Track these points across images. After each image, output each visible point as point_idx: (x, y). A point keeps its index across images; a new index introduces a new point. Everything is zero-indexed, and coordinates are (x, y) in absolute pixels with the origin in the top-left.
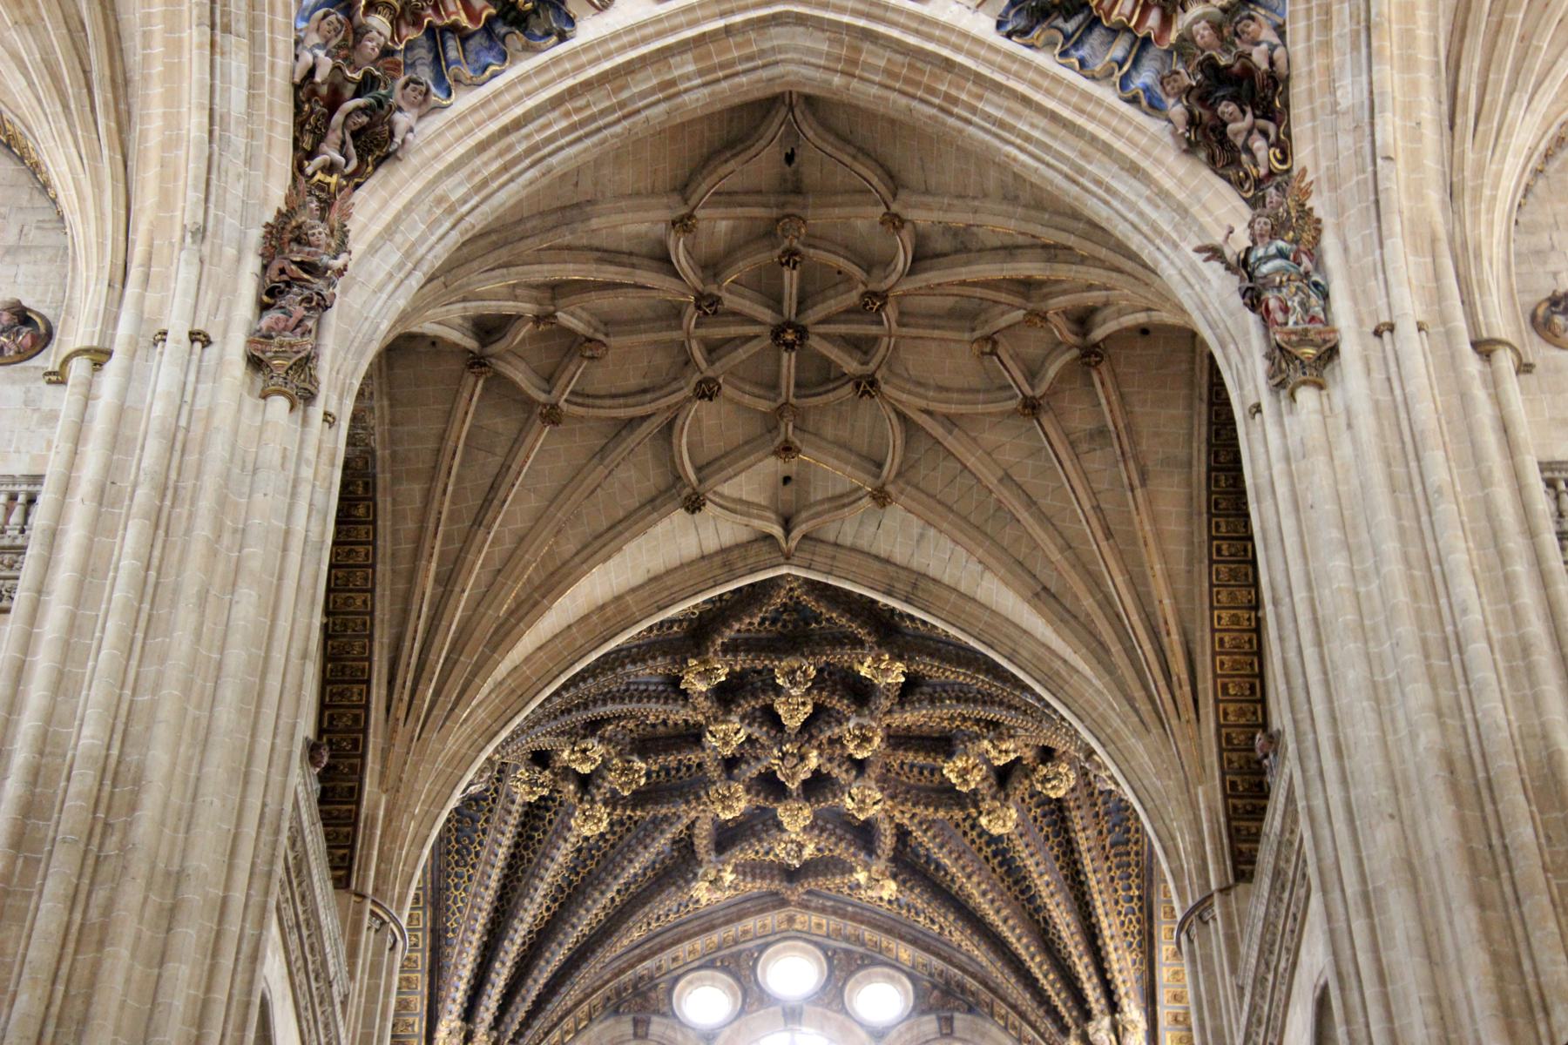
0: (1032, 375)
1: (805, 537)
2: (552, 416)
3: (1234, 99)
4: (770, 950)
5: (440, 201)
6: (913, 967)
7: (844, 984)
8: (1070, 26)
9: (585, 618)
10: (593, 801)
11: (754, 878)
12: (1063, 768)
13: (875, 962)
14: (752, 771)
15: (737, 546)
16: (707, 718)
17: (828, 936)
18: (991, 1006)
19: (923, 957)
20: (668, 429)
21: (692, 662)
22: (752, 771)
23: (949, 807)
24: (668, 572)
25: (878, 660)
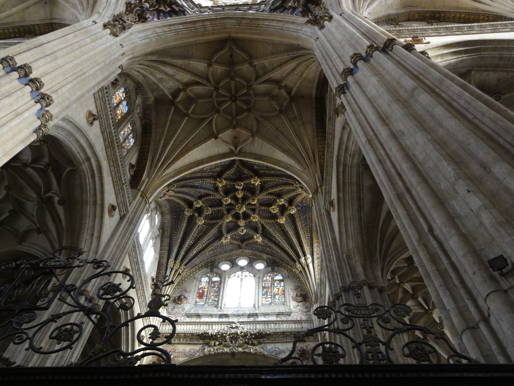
0: (281, 106)
1: (239, 151)
2: (187, 115)
3: (311, 3)
5: (155, 31)
8: (281, 10)
9: (195, 162)
12: (293, 207)
13: (259, 260)
14: (233, 212)
16: (223, 197)
17: (250, 255)
18: (282, 264)
20: (210, 122)
21: (218, 179)
22: (233, 212)
23: (272, 220)
24: (212, 157)
25: (255, 178)
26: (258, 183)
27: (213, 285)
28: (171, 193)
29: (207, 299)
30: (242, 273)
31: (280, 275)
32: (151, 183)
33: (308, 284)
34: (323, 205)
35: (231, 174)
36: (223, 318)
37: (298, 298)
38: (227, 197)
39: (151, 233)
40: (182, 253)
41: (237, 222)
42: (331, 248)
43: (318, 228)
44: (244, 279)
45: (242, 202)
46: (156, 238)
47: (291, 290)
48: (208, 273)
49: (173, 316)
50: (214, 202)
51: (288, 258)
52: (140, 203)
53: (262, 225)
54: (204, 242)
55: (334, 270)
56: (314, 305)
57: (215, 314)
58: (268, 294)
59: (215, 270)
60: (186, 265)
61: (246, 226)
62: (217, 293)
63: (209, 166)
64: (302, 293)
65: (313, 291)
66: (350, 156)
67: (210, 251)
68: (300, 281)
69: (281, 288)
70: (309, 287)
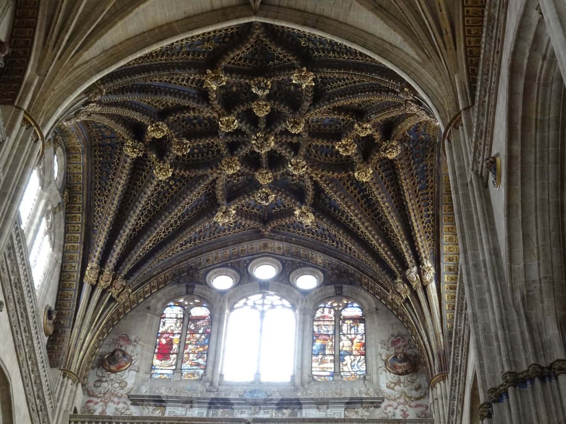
4: (255, 261)
6: (324, 267)
7: (290, 273)
9: (151, 30)
10: (165, 162)
11: (246, 218)
12: (394, 143)
13: (305, 265)
14: (244, 151)
15: (230, 7)
16: (219, 115)
17: (283, 255)
18: (360, 280)
19: (328, 259)
21: (209, 71)
22: (244, 151)
23: (339, 172)
24: (195, 16)
25: (300, 71)
26: (308, 83)
27: (192, 327)
28: (92, 108)
29: (180, 361)
30: (263, 298)
31: (355, 305)
32: (47, 87)
33: (423, 332)
34: (471, 163)
35: (241, 58)
36: (218, 408)
37: (399, 364)
38: (229, 114)
39: (43, 202)
40: (118, 249)
41: (253, 175)
42: (486, 272)
43: (453, 196)
44: (269, 313)
45: (266, 128)
46: (55, 213)
47: (383, 343)
48: (180, 296)
49: (99, 400)
50: (197, 126)
51: (376, 267)
52: (23, 142)
53: (316, 184)
54: (172, 221)
55: (493, 330)
56: (438, 385)
57: (198, 398)
58: (327, 352)
59: (198, 289)
60: (126, 278)
61: (275, 186)
62: (202, 346)
63: (187, 39)
64: (409, 352)
65: (435, 352)
66: (544, 58)
67: (186, 242)
68: (404, 322)
69: (359, 337)
70: (425, 339)
